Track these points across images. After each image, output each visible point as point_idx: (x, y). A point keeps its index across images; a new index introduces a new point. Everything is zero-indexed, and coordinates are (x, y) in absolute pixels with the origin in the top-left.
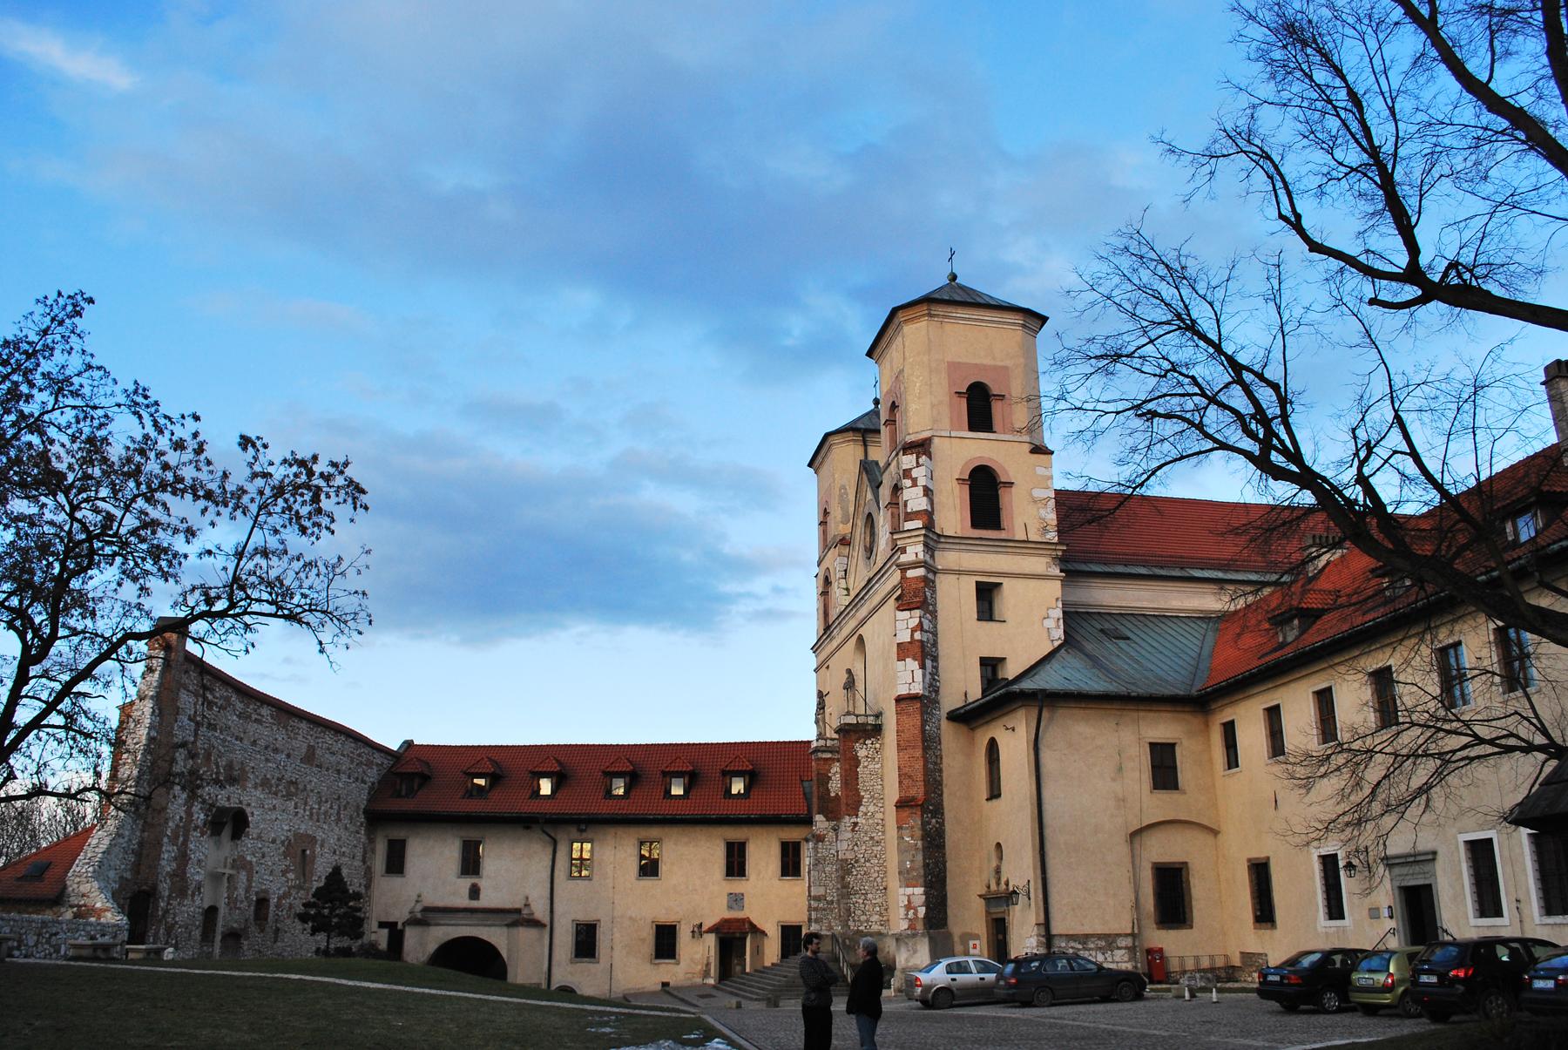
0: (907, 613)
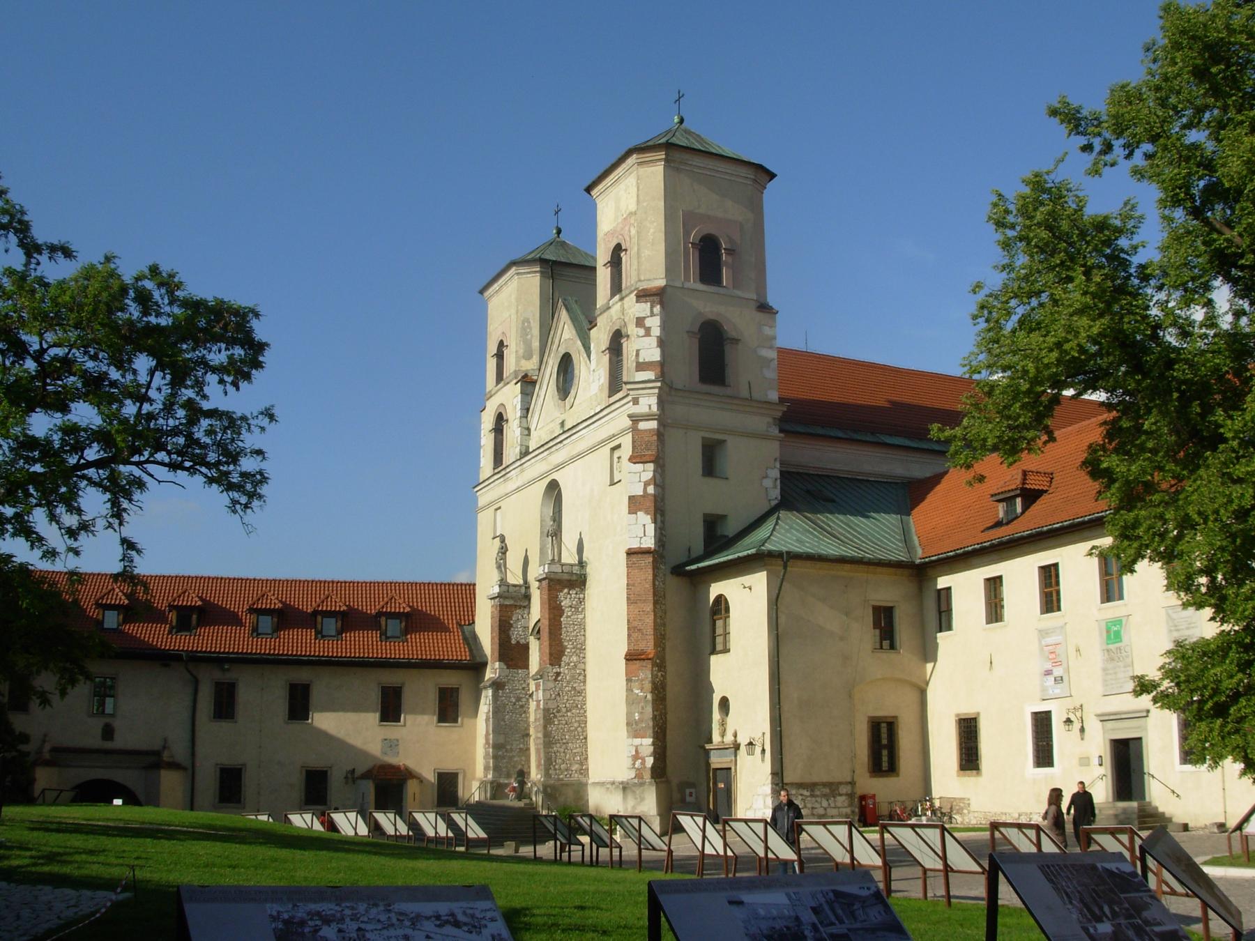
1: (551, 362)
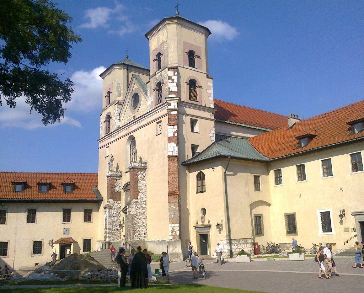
1: (129, 97)
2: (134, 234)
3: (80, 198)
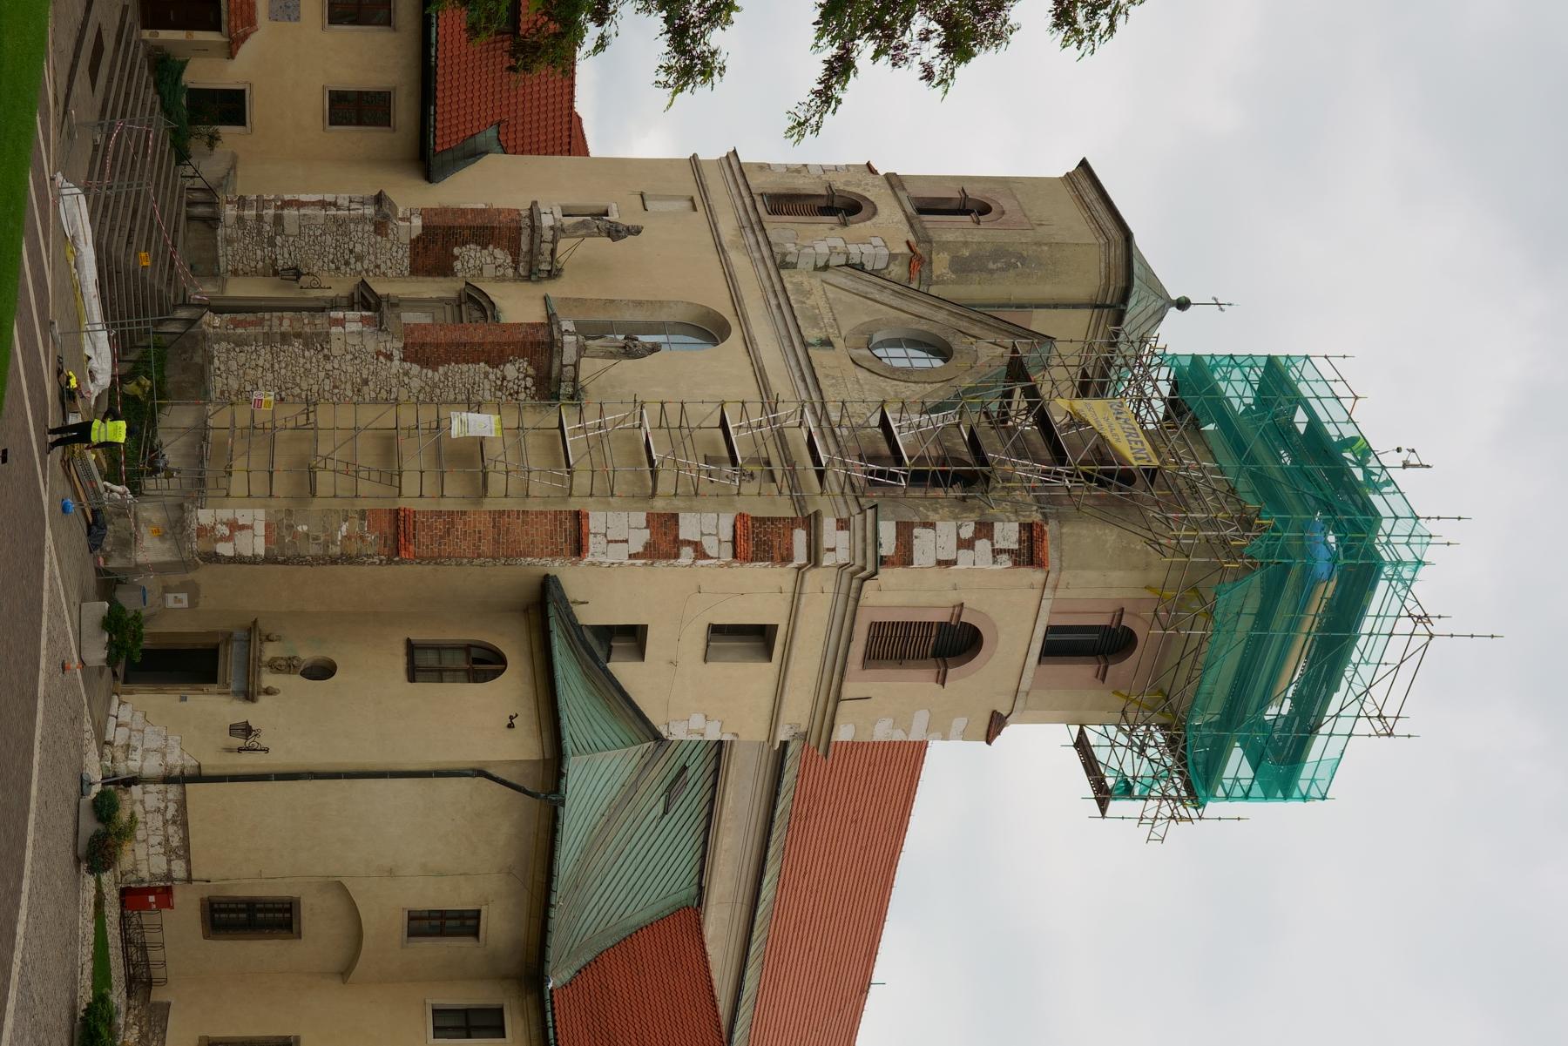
0: (727, 534)
1: (941, 316)
2: (240, 343)
3: (440, 72)
